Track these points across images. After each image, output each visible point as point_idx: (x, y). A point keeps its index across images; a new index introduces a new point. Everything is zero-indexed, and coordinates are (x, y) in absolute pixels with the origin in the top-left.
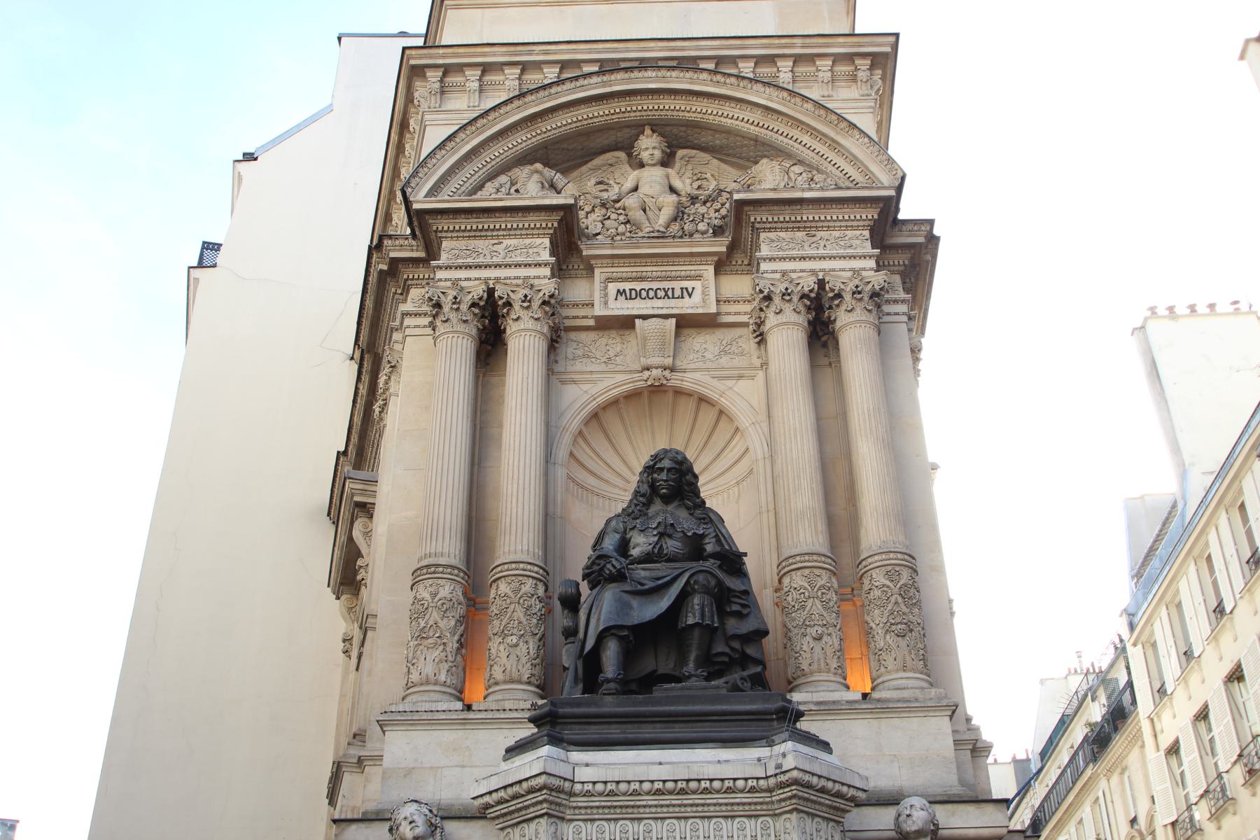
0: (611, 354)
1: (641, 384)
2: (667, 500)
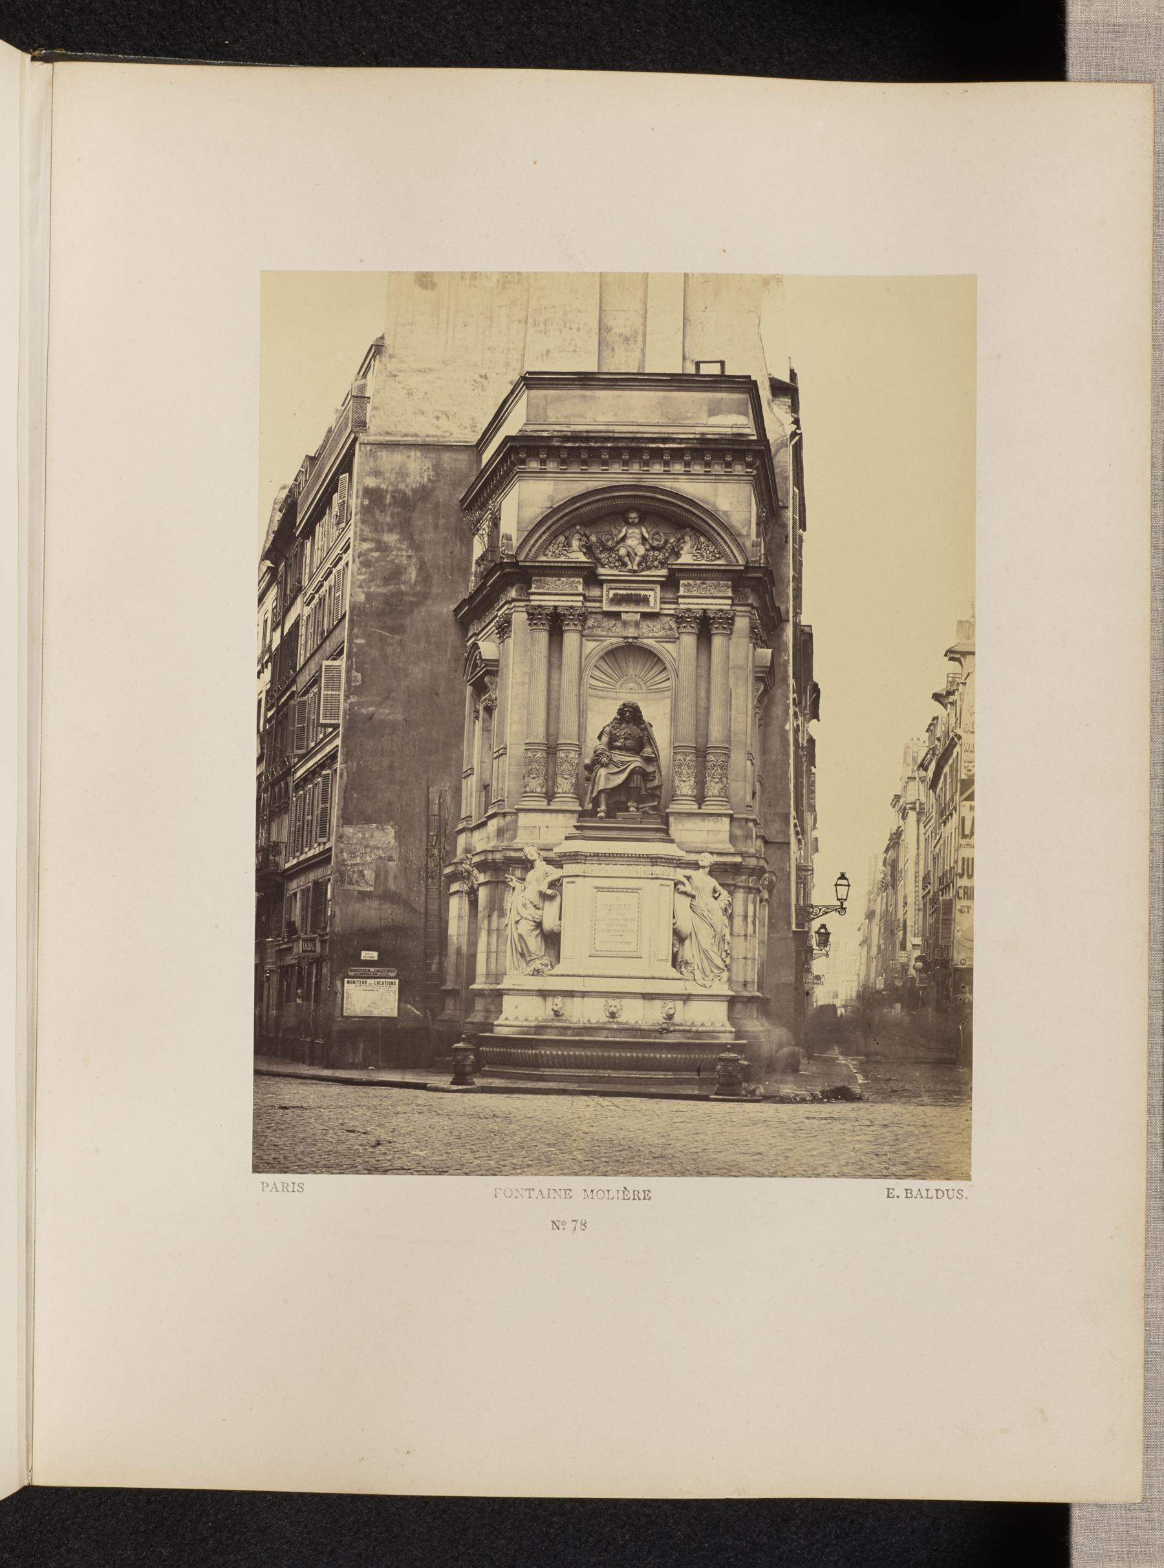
0: (610, 625)
1: (623, 644)
2: (628, 723)
